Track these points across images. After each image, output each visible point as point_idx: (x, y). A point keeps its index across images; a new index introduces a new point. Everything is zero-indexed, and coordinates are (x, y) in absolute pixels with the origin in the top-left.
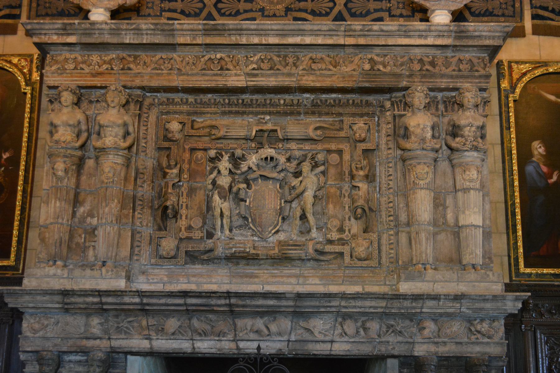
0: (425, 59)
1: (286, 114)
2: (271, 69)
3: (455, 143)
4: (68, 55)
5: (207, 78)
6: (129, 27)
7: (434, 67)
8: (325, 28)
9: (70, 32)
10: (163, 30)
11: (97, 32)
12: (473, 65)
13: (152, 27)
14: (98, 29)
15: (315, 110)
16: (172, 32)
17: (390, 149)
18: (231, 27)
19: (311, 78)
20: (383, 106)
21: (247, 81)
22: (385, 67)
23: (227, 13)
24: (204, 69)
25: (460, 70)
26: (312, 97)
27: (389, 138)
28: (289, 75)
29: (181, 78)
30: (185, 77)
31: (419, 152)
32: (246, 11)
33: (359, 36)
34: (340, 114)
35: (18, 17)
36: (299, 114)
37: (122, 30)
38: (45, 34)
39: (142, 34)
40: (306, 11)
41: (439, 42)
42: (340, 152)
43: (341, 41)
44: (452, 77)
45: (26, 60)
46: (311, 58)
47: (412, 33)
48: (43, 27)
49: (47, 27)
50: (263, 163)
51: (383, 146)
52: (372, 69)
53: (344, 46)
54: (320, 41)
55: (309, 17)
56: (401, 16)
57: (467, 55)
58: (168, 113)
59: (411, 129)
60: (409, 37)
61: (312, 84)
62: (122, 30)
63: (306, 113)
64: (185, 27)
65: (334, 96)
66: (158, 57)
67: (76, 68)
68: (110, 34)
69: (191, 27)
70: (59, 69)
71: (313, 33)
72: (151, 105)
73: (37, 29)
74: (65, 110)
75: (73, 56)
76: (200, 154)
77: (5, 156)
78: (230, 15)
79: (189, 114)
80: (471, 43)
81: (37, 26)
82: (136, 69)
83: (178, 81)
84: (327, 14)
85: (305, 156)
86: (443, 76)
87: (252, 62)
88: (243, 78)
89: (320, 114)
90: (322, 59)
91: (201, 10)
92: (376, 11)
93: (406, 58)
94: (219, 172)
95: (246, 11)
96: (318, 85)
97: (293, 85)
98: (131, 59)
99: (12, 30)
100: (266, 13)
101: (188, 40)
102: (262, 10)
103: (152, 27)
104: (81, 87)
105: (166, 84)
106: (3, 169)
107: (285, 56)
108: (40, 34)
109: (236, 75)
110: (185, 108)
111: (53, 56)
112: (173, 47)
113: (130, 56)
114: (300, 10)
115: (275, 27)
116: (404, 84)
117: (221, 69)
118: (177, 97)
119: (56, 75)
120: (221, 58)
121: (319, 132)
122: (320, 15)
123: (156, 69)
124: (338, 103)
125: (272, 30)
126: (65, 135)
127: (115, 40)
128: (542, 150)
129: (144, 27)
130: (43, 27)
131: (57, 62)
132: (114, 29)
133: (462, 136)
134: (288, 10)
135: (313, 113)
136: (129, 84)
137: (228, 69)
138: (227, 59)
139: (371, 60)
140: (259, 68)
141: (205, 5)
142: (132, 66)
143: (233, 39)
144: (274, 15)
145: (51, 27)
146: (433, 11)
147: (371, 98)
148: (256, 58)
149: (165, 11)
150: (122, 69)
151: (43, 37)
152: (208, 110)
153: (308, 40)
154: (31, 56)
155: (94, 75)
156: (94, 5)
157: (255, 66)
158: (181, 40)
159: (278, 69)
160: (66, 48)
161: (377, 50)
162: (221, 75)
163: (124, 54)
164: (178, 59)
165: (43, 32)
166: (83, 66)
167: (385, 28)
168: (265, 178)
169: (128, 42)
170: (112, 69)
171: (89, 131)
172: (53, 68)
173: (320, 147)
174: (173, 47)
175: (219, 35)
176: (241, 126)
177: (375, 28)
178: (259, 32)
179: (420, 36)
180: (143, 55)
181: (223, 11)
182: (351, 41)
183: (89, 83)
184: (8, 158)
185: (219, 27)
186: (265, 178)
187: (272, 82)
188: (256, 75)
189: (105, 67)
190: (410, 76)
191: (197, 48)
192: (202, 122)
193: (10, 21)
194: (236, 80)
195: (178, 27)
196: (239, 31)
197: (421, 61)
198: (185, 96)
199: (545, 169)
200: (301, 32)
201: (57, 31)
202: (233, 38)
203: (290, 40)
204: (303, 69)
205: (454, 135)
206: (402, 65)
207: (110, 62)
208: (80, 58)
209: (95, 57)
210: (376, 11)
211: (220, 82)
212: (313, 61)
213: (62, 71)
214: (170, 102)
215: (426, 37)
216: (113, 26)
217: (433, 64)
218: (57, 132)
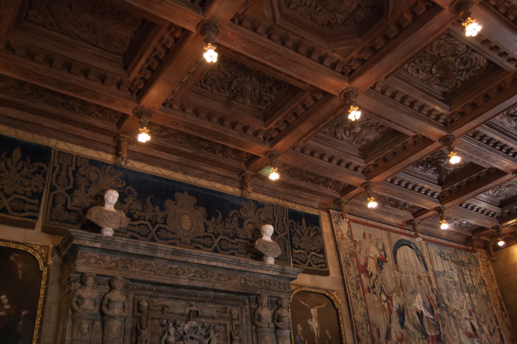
0: (266, 281)
1: (200, 301)
2: (200, 277)
3: (280, 324)
4: (91, 254)
5: (169, 278)
6: (133, 244)
7: (270, 285)
8: (229, 260)
9: (98, 241)
10: (151, 248)
11: (114, 243)
12: (285, 286)
13: (146, 246)
14: (116, 242)
15: (214, 300)
16: (155, 249)
17: (248, 325)
18: (186, 252)
19: (219, 285)
20: (245, 302)
21: (189, 283)
22: (250, 283)
23: (162, 238)
24: (167, 273)
25: (280, 288)
26: (214, 293)
27: (248, 319)
28: (210, 282)
29: (156, 277)
30: (158, 277)
31: (267, 329)
32: (172, 239)
33: (242, 266)
34: (225, 304)
35: (36, 218)
36: (206, 302)
37: (129, 244)
38: (82, 240)
39: (139, 249)
40: (200, 243)
41: (274, 274)
42: (225, 325)
43: (234, 267)
44: (277, 291)
45: (45, 249)
46: (219, 274)
47: (264, 268)
48: (83, 235)
49: (85, 236)
50: (192, 330)
51: (244, 323)
52: (245, 283)
53: (233, 269)
54: (225, 266)
55: (202, 247)
56: (243, 253)
57: (282, 281)
58: (139, 295)
59: (263, 316)
60: (262, 269)
61: (219, 288)
62: (129, 244)
63: (209, 302)
64: (164, 249)
65: (223, 294)
66: (143, 262)
67: (96, 263)
68: (121, 246)
69: (167, 249)
70: (85, 262)
71: (223, 261)
72: (132, 289)
73: (78, 236)
74: (88, 289)
75: (94, 255)
76: (156, 322)
77: (24, 313)
78: (163, 239)
79: (151, 296)
80: (286, 276)
81: (78, 234)
82: (133, 269)
83: (154, 278)
84: (210, 247)
85: (210, 326)
86: (274, 290)
87: (191, 272)
88: (187, 280)
89: (216, 303)
90: (223, 275)
91: (149, 234)
92: (232, 249)
93: (259, 280)
94: (169, 334)
95: (172, 239)
96: (222, 289)
97: (211, 287)
98: (128, 262)
99: (32, 226)
100: (182, 241)
101: (162, 256)
102: (180, 239)
103: (146, 246)
104: (97, 275)
105: (147, 279)
106: (22, 322)
107: (207, 271)
108: (79, 239)
109: (184, 279)
110: (149, 293)
111: (82, 253)
112: (152, 258)
113: (128, 260)
114: (198, 243)
115: (207, 256)
116: (259, 292)
117: (176, 274)
118: (147, 286)
119: (84, 265)
120: (176, 268)
121: (218, 314)
122: (207, 247)
123: (142, 269)
124: (225, 298)
125: (205, 257)
126: (88, 305)
127: (123, 250)
128: (301, 329)
129: (142, 245)
130: (83, 235)
131: (84, 257)
132: (125, 244)
133: (283, 322)
134: (192, 242)
135: (213, 302)
136: (127, 277)
137: (179, 275)
138: (179, 269)
139: (245, 278)
140: (195, 276)
141: (150, 232)
142: (129, 266)
143: (185, 259)
144: (186, 243)
145: (88, 236)
146: (267, 257)
147: (240, 297)
148: (193, 270)
149: (129, 231)
150: (123, 267)
151: (80, 241)
152: (162, 295)
153: (220, 265)
154: (48, 247)
155: (107, 269)
156: (107, 225)
157: (192, 275)
158: (159, 255)
159: (204, 278)
160: (90, 249)
161: (247, 274)
162: (176, 278)
163: (124, 258)
164: (154, 265)
165: (81, 238)
166: (101, 262)
167: (254, 264)
168: (192, 338)
169: (130, 252)
170: (117, 266)
171: (103, 304)
172: (82, 261)
173: (216, 322)
174: (152, 258)
175: (179, 255)
176: (179, 307)
177: (250, 263)
178: (199, 257)
179: (267, 270)
180: (136, 261)
181: (160, 236)
182: (238, 268)
183: (103, 273)
184: (25, 315)
185: (181, 252)
186: (192, 338)
187: (201, 284)
188: (193, 280)
189: (113, 264)
190: (261, 289)
191: (164, 260)
192: (157, 302)
193: (31, 220)
194: (184, 281)
195: (160, 248)
196: (189, 255)
197: (265, 281)
198: (151, 286)
199: (303, 339)
200: (217, 260)
201: (90, 239)
202: (185, 258)
203: (212, 263)
204: (216, 279)
205: (278, 321)
206: (257, 282)
207: (116, 262)
208: (98, 257)
209: (108, 258)
210: (232, 249)
211: (176, 281)
212: (219, 275)
213: (87, 263)
214: (143, 289)
215: (269, 270)
216: (125, 242)
217: (269, 283)
218: (83, 302)
